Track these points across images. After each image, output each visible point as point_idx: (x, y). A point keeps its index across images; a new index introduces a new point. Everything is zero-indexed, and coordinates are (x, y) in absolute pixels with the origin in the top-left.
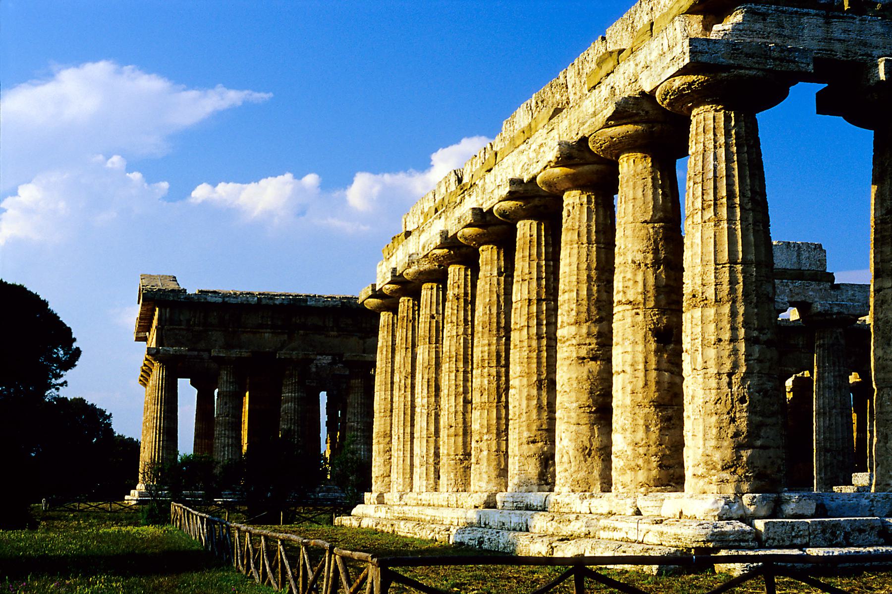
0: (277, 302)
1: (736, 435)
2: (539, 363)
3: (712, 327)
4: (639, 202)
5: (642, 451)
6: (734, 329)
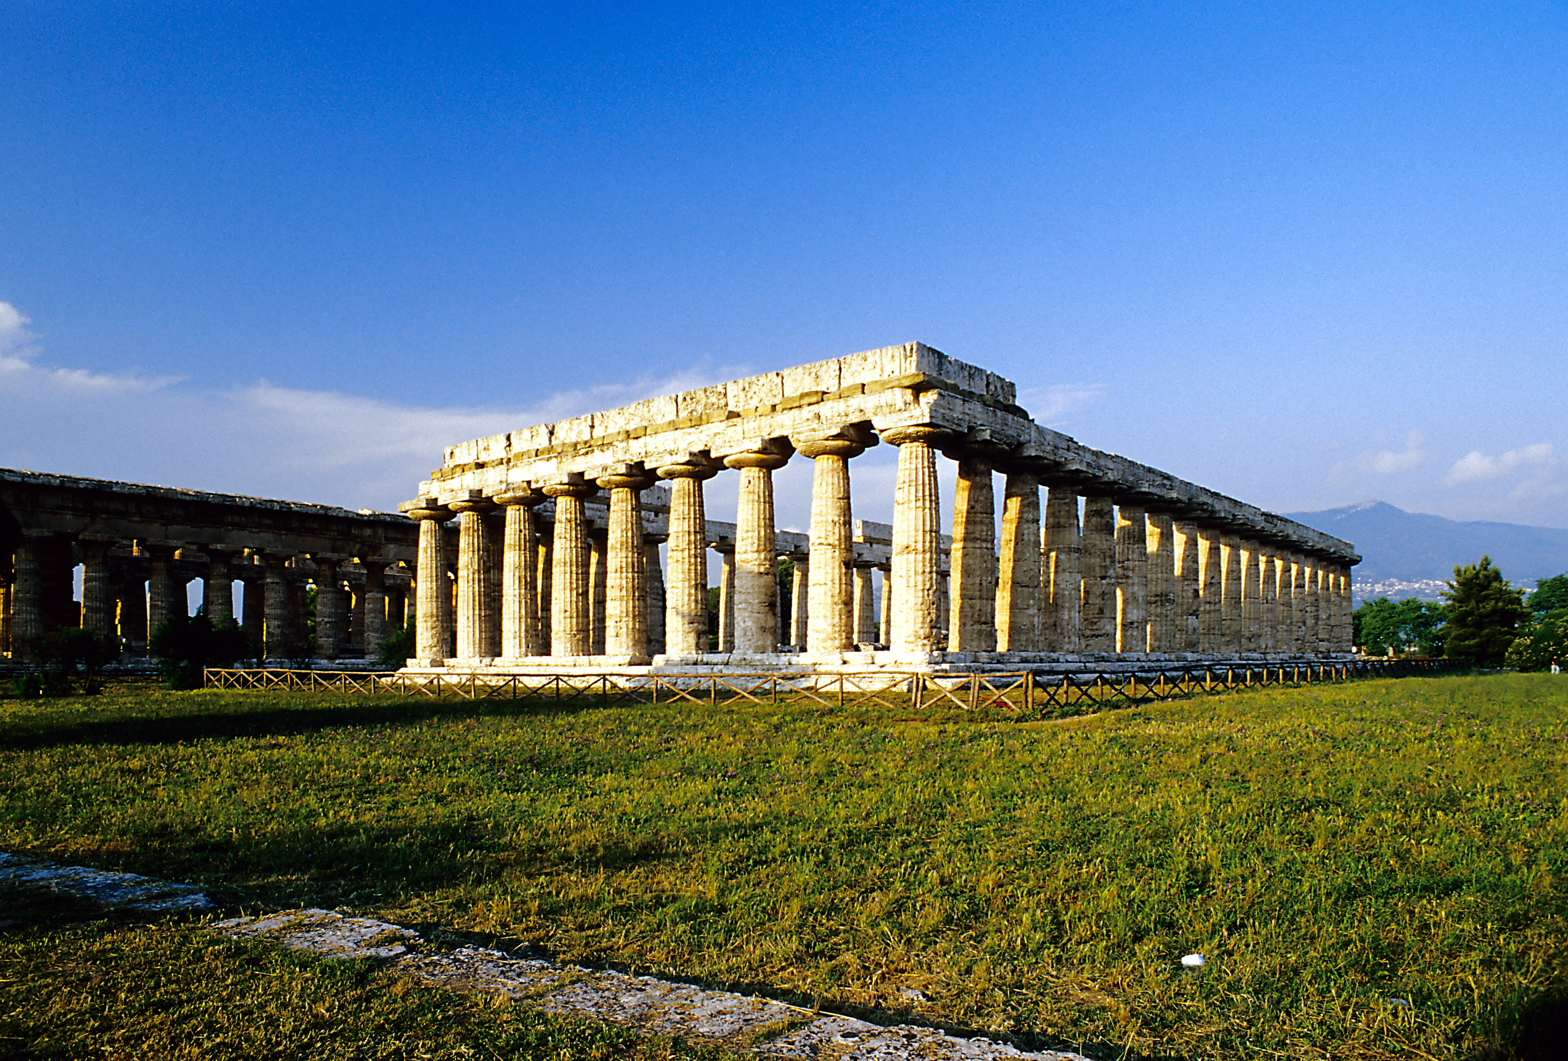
0: (81, 486)
1: (931, 621)
2: (696, 573)
3: (921, 564)
4: (836, 486)
5: (837, 629)
6: (931, 567)
